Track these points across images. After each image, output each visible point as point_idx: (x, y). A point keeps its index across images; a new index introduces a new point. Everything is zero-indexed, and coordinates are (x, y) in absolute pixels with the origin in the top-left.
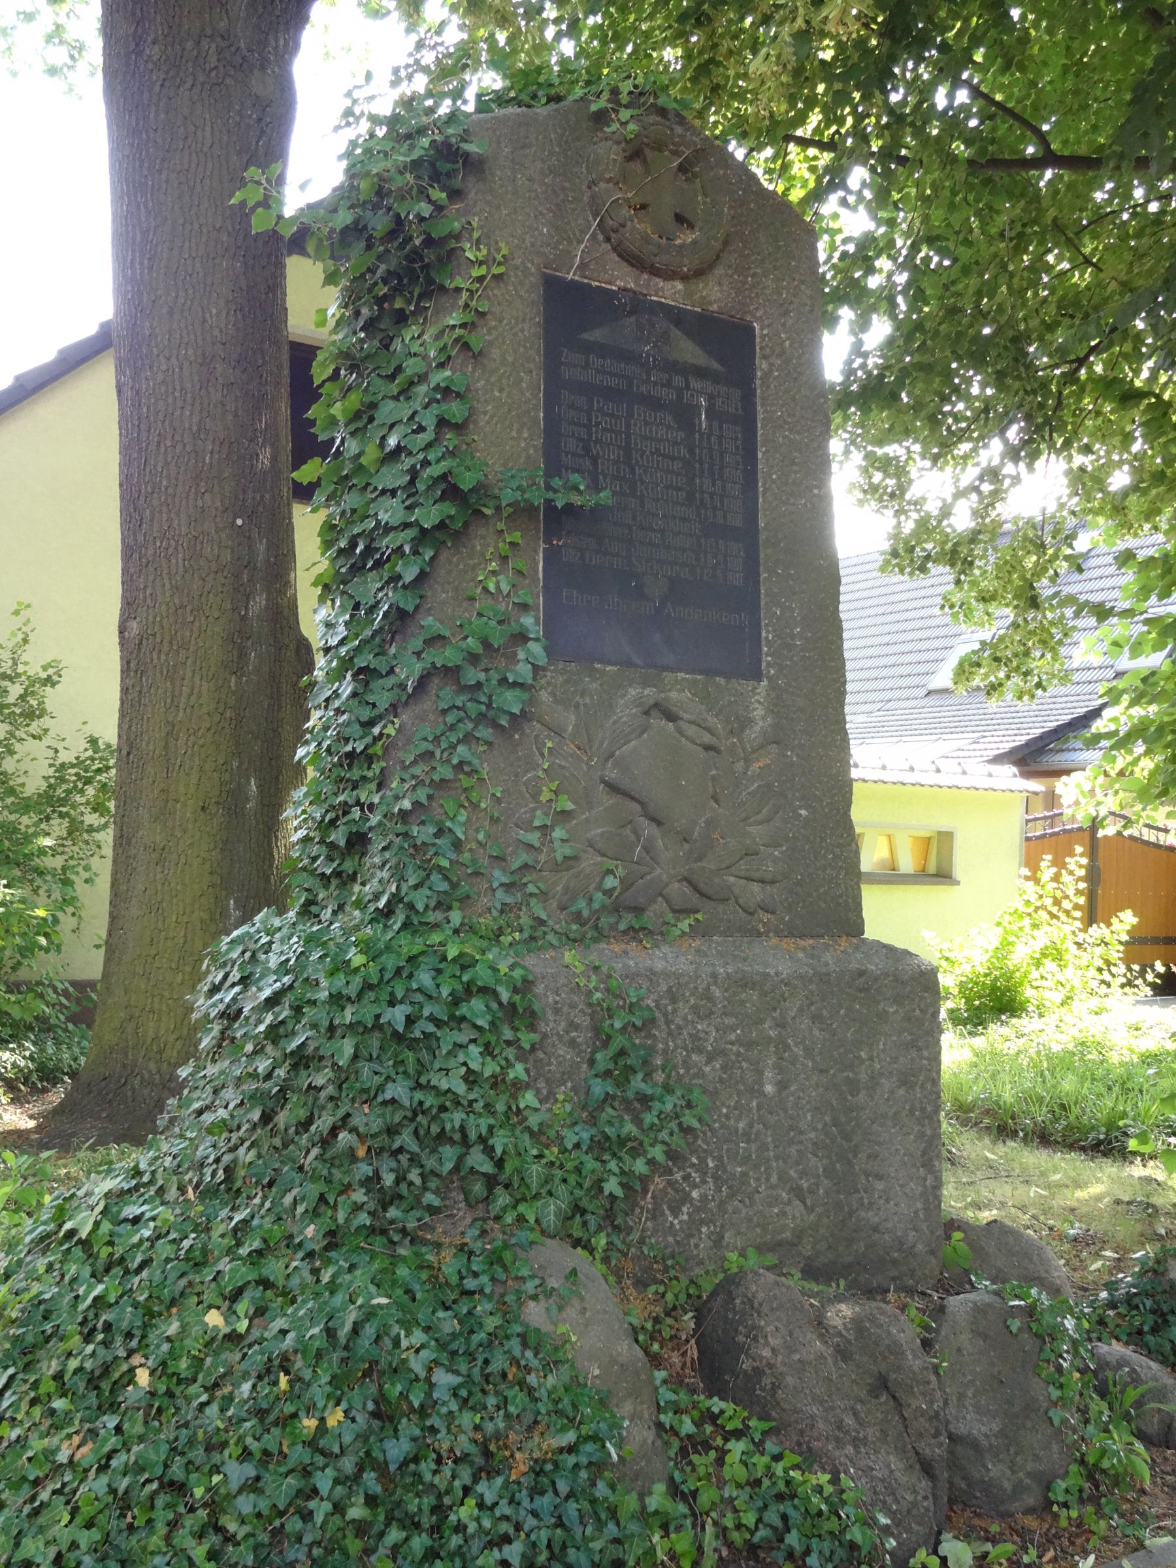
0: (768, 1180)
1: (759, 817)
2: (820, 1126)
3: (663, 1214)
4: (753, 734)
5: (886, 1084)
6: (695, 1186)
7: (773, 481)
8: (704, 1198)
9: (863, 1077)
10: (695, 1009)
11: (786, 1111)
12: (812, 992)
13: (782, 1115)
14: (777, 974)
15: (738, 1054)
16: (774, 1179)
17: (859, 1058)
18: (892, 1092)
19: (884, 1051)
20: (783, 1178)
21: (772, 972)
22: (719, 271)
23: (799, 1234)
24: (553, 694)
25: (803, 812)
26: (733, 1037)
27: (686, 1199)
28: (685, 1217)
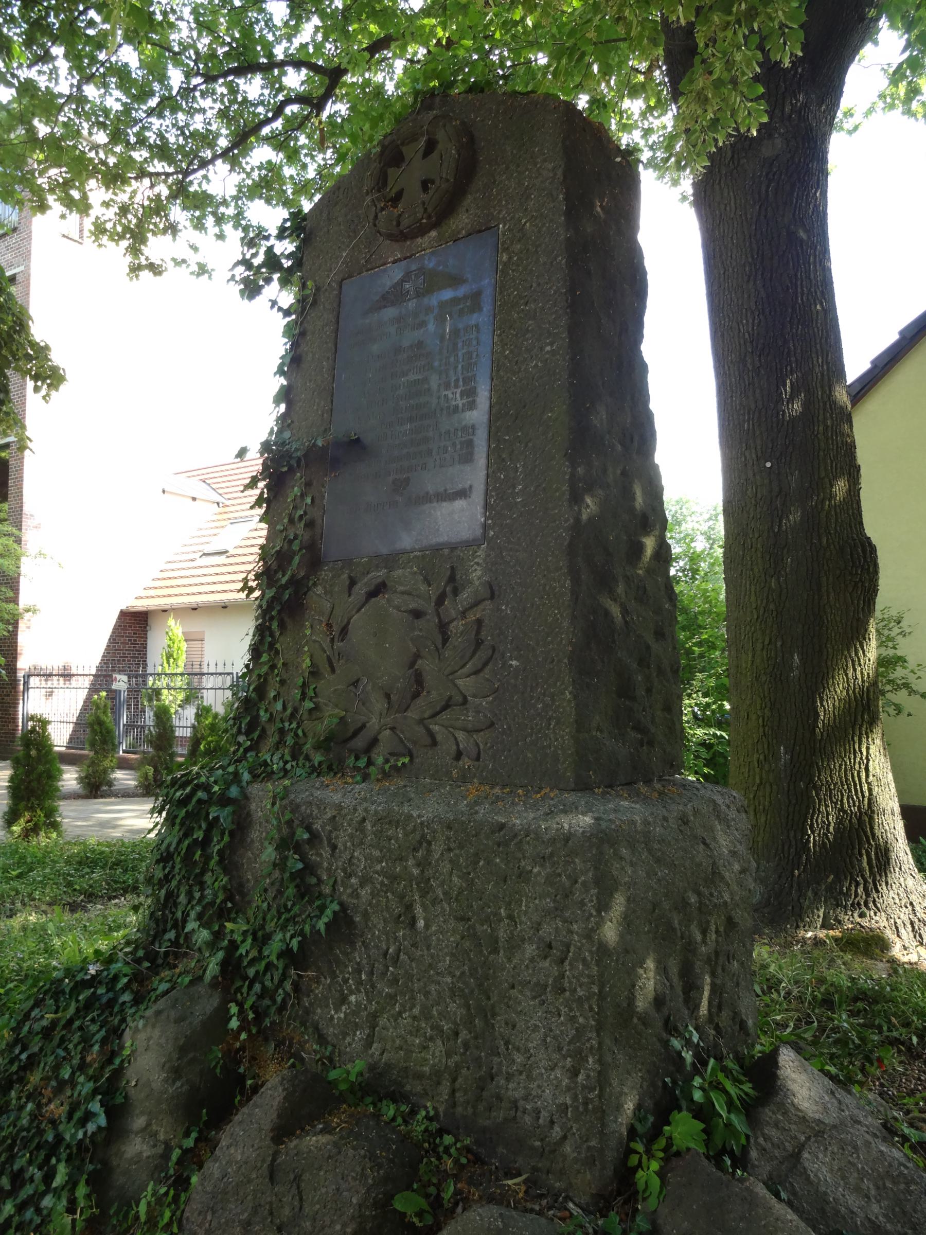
0: (411, 1009)
1: (465, 670)
2: (458, 973)
3: (327, 1006)
4: (465, 596)
5: (530, 950)
6: (352, 992)
7: (506, 357)
8: (358, 1004)
9: (502, 934)
10: (351, 836)
11: (428, 948)
12: (448, 838)
13: (426, 952)
14: (419, 816)
15: (382, 883)
16: (416, 1011)
17: (496, 914)
18: (532, 960)
19: (526, 912)
20: (426, 1014)
21: (415, 813)
22: (469, 200)
23: (437, 1076)
24: (325, 588)
25: (514, 663)
26: (378, 867)
27: (344, 1000)
28: (342, 1015)
